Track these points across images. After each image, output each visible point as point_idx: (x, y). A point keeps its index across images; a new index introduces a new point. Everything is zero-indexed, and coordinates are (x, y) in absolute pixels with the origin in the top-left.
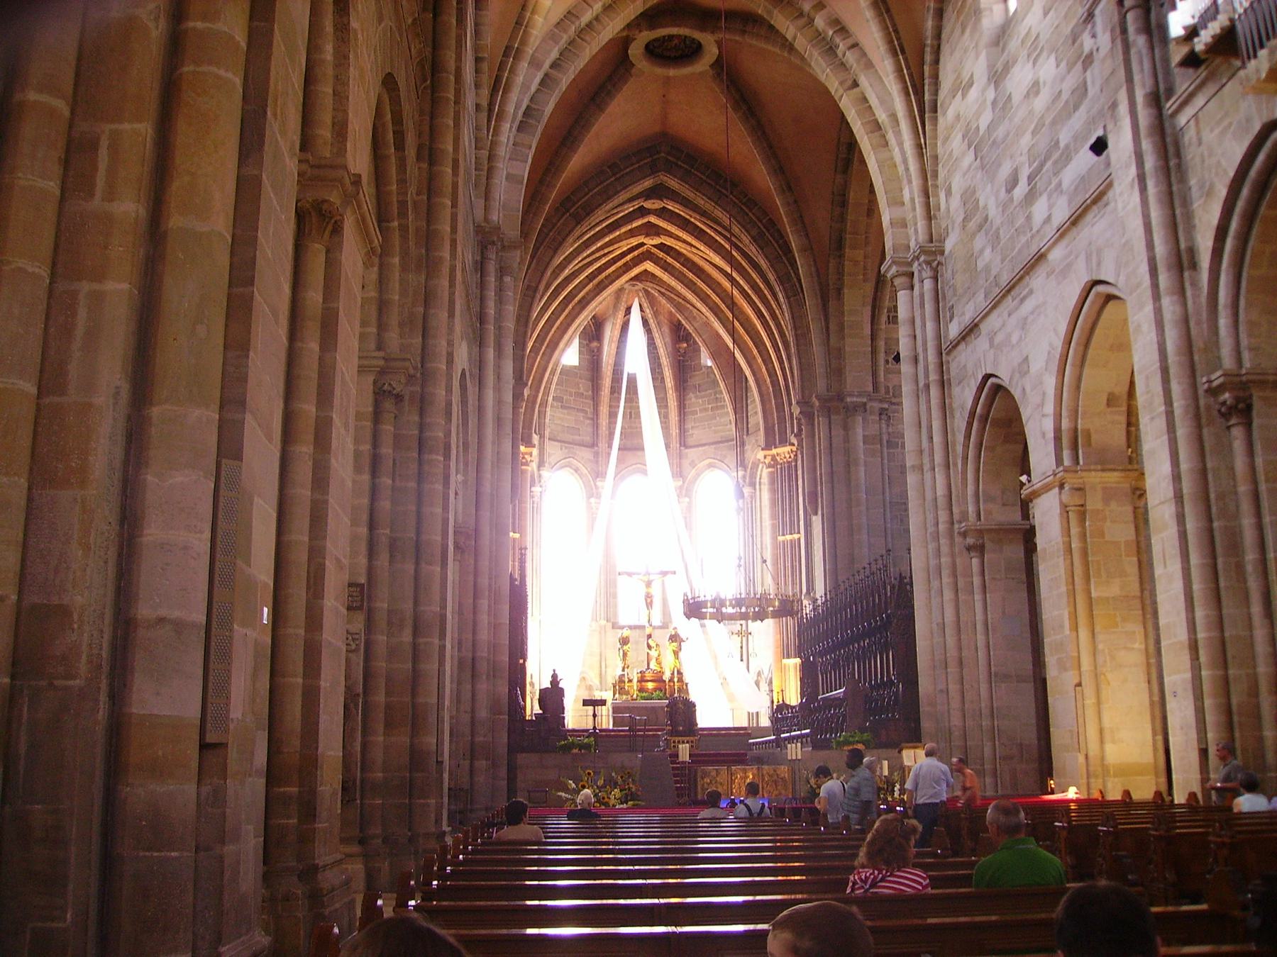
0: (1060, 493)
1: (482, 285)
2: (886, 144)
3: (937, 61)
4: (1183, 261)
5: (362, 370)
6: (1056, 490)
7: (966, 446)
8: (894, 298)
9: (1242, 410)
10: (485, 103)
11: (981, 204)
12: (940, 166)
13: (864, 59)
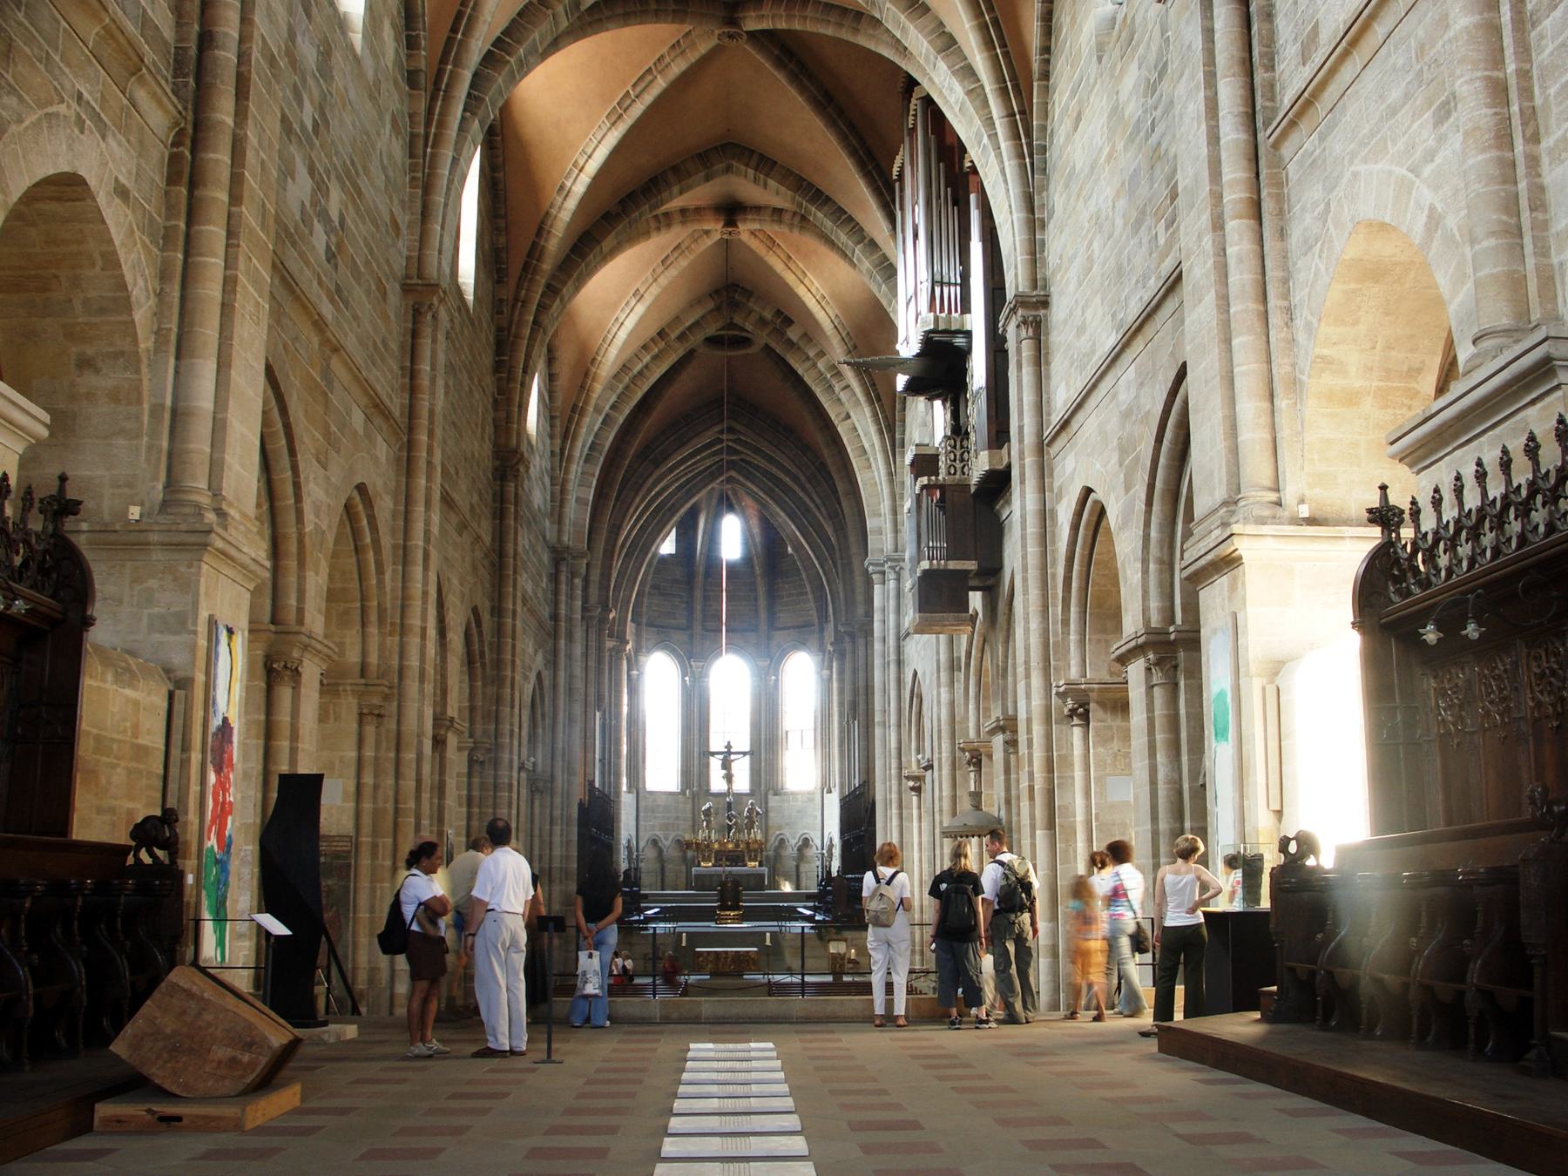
1: (556, 593)
2: (870, 467)
3: (904, 409)
4: (953, 666)
5: (460, 749)
7: (910, 712)
10: (557, 450)
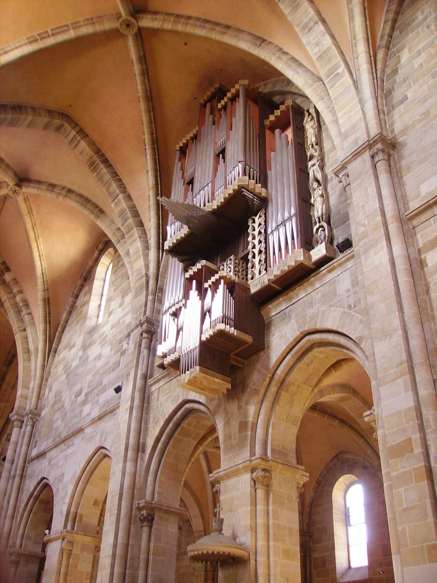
0: (62, 542)
2: (30, 360)
3: (63, 332)
4: (140, 448)
6: (60, 540)
7: (24, 510)
8: (12, 430)
9: (149, 520)
11: (63, 399)
12: (50, 376)
13: (32, 321)
